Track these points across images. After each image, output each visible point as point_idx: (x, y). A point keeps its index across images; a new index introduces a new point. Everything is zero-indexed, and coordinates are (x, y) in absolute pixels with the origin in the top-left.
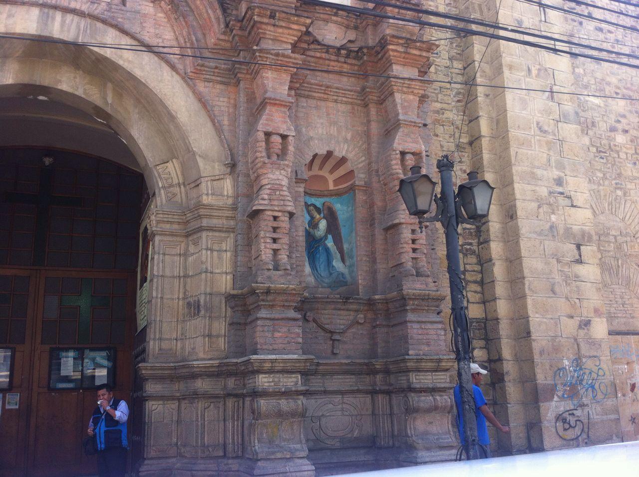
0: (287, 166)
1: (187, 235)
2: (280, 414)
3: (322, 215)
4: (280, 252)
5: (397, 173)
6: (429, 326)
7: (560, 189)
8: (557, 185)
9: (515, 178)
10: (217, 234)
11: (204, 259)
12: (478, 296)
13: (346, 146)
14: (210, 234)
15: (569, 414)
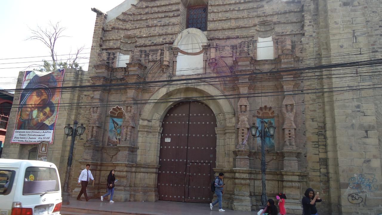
0: (247, 114)
1: (225, 134)
2: (241, 184)
3: (268, 124)
4: (244, 140)
5: (284, 112)
6: (291, 161)
7: (359, 110)
8: (357, 108)
9: (335, 108)
10: (230, 134)
11: (227, 141)
12: (323, 150)
13: (271, 104)
14: (228, 134)
15: (356, 194)
